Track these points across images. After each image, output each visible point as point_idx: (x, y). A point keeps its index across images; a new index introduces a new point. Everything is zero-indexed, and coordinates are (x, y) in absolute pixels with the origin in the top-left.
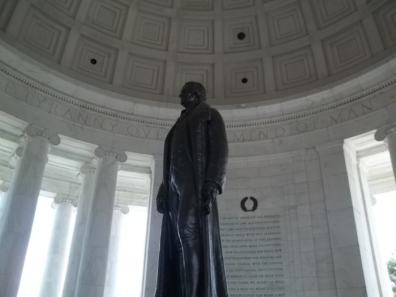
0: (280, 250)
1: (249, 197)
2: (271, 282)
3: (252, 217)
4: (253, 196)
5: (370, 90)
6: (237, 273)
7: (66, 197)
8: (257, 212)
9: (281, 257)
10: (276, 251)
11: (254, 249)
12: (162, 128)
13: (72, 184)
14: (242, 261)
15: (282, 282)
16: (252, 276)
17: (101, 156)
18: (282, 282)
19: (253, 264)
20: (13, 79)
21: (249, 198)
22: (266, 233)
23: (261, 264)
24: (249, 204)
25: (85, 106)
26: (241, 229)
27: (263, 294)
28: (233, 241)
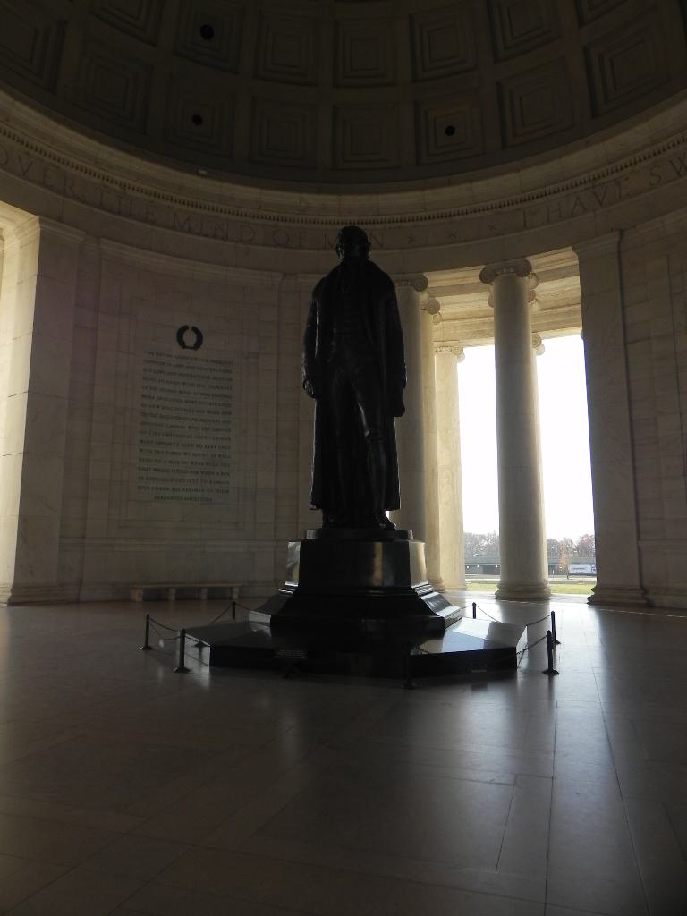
0: (230, 413)
1: (191, 325)
4: (197, 326)
5: (388, 218)
8: (200, 352)
9: (229, 422)
10: (223, 413)
19: (190, 427)
24: (190, 338)
26: (174, 374)
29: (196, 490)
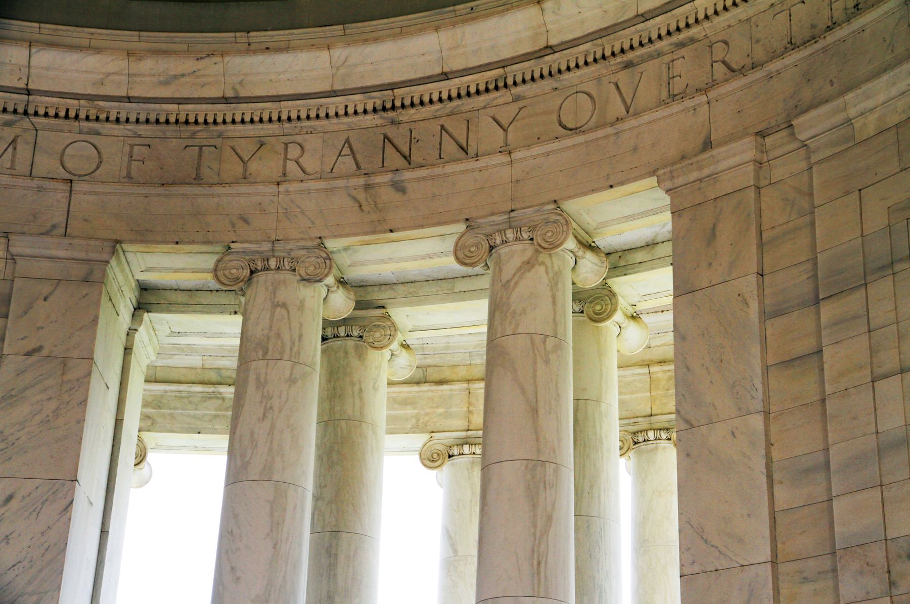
7: (643, 424)
12: (682, 45)
13: (654, 369)
17: (467, 261)
20: (142, 129)
25: (389, 101)
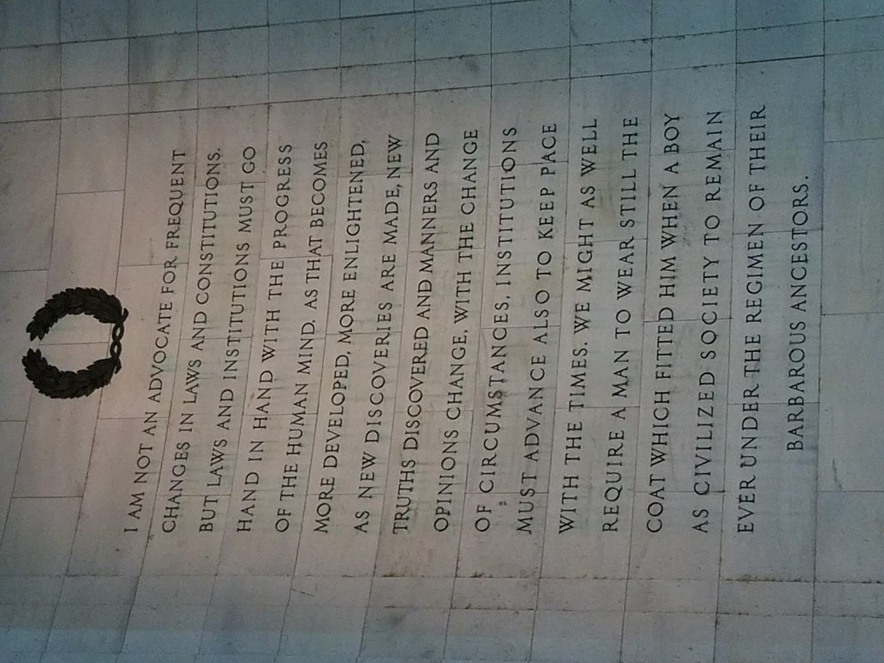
1: (25, 343)
2: (585, 203)
3: (164, 322)
6: (514, 416)
11: (365, 313)
14: (436, 386)
15: (588, 133)
16: (541, 321)
18: (588, 133)
19: (461, 315)
21: (35, 345)
22: (279, 233)
23: (466, 265)
24: (78, 342)
26: (228, 397)
27: (658, 254)
28: (294, 449)
29: (755, 262)
